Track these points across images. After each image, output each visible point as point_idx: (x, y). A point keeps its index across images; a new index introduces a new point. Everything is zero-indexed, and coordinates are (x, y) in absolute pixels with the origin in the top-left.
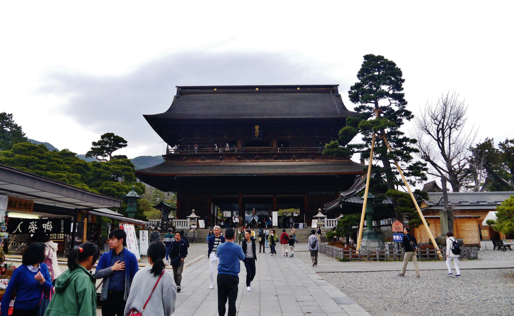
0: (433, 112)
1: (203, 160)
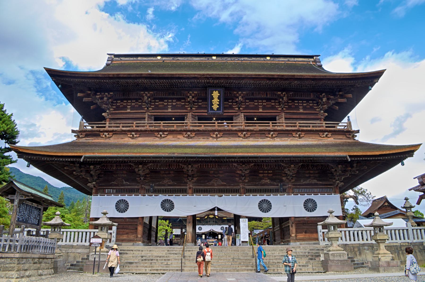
1: (133, 138)
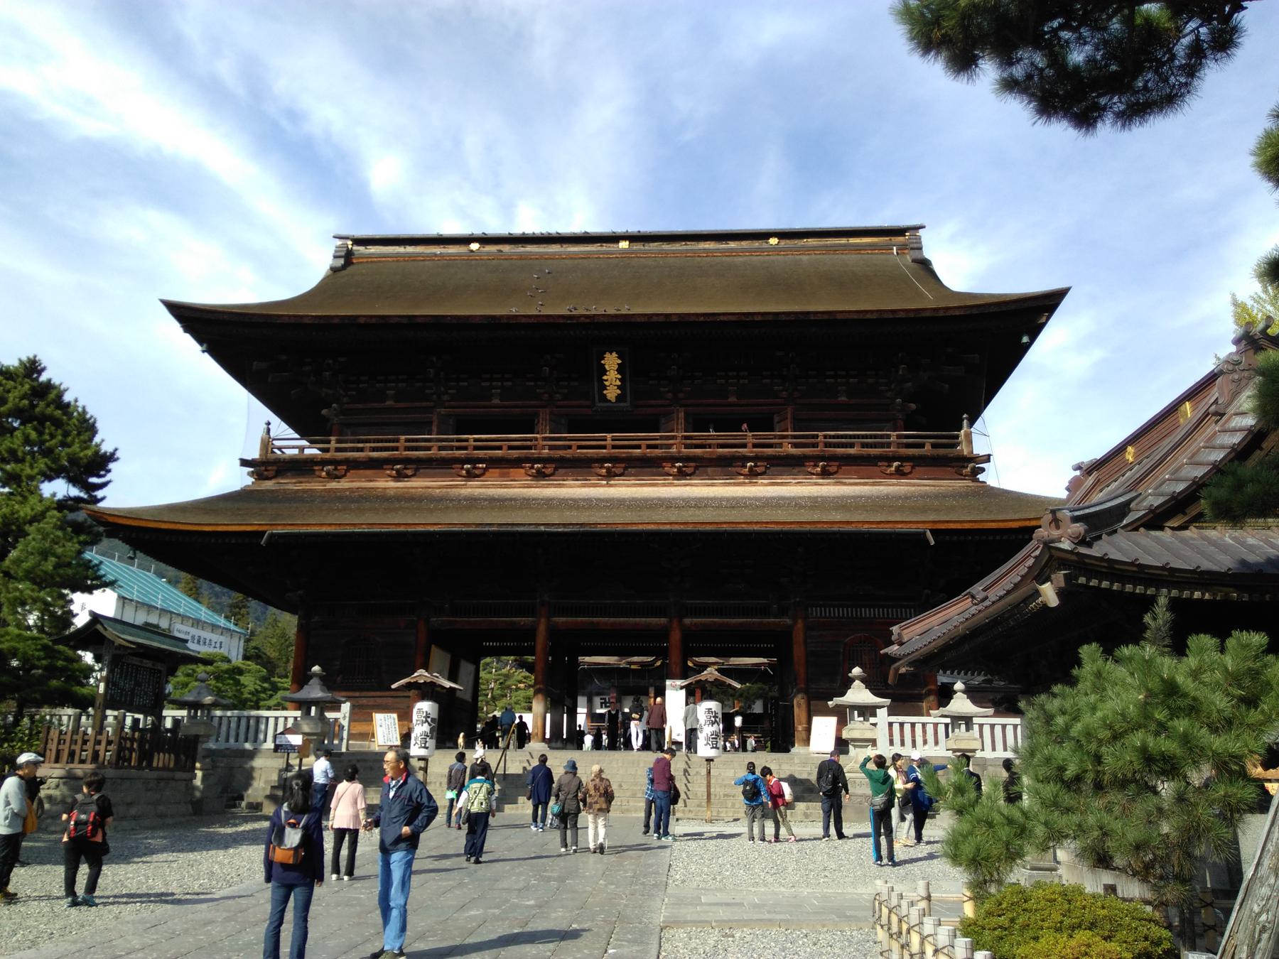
1: (400, 476)
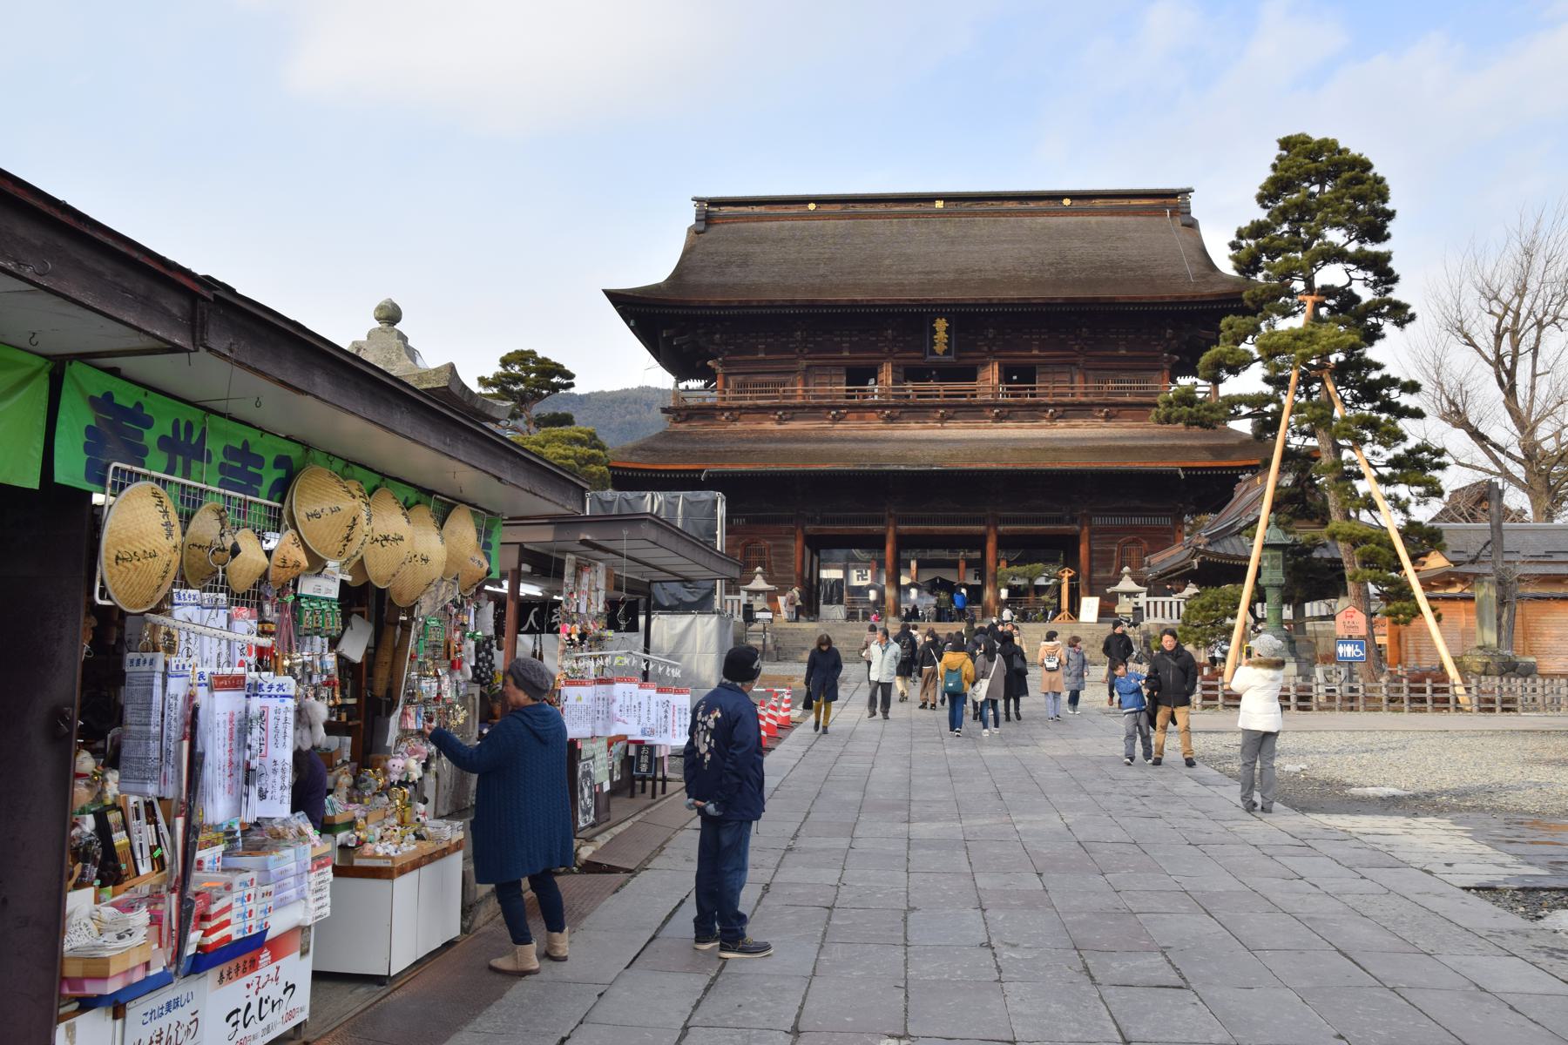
0: (1488, 275)
1: (780, 421)
